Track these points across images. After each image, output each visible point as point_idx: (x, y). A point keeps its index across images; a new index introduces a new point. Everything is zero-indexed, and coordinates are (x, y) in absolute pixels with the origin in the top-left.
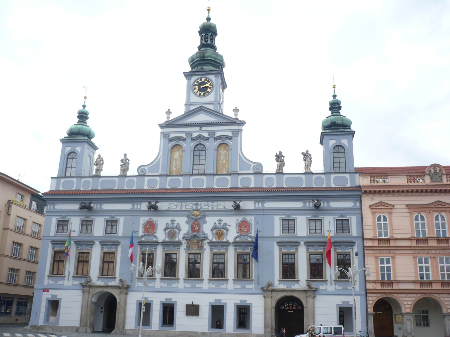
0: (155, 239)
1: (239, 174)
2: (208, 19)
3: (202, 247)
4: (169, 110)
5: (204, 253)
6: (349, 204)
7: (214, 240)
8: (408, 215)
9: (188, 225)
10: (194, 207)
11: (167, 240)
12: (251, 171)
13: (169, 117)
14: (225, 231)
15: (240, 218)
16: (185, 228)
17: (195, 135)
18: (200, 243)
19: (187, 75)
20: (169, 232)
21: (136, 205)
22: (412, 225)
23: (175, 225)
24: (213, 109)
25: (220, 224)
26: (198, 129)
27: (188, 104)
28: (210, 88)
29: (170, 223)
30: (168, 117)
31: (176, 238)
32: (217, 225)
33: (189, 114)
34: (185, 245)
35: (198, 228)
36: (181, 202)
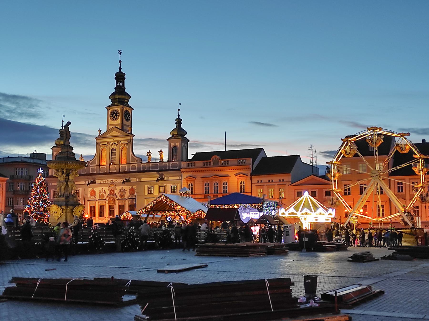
0: (95, 199)
1: (130, 164)
2: (120, 69)
3: (115, 202)
4: (100, 129)
5: (115, 205)
6: (177, 178)
7: (120, 198)
8: (202, 183)
9: (109, 191)
10: (111, 182)
11: (100, 199)
12: (136, 162)
13: (100, 133)
14: (124, 194)
15: (131, 187)
16: (108, 192)
17: (111, 143)
18: (114, 200)
19: (108, 108)
20: (101, 195)
21: (86, 182)
22: (203, 188)
23: (103, 191)
24: (119, 128)
25: (122, 189)
26: (112, 140)
27: (108, 125)
28: (118, 116)
29: (101, 190)
30: (100, 133)
31: (103, 198)
32: (121, 190)
33: (109, 131)
34: (108, 201)
35: (112, 193)
36: (106, 179)
